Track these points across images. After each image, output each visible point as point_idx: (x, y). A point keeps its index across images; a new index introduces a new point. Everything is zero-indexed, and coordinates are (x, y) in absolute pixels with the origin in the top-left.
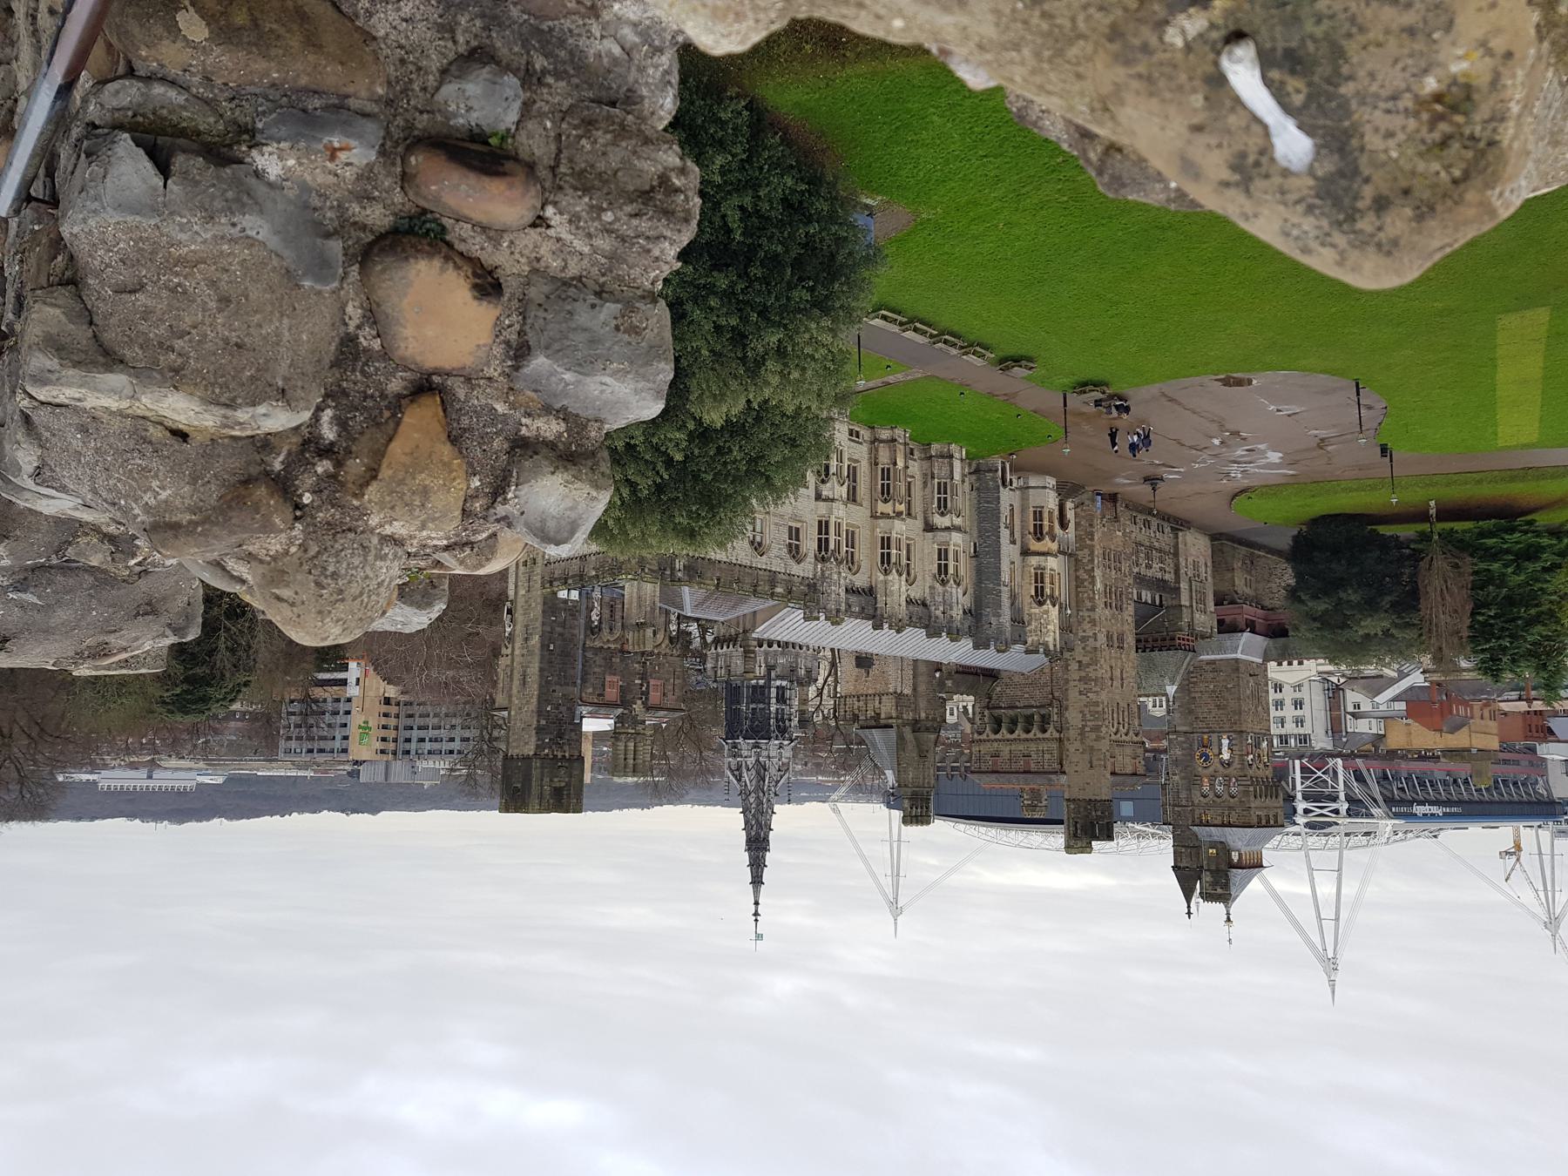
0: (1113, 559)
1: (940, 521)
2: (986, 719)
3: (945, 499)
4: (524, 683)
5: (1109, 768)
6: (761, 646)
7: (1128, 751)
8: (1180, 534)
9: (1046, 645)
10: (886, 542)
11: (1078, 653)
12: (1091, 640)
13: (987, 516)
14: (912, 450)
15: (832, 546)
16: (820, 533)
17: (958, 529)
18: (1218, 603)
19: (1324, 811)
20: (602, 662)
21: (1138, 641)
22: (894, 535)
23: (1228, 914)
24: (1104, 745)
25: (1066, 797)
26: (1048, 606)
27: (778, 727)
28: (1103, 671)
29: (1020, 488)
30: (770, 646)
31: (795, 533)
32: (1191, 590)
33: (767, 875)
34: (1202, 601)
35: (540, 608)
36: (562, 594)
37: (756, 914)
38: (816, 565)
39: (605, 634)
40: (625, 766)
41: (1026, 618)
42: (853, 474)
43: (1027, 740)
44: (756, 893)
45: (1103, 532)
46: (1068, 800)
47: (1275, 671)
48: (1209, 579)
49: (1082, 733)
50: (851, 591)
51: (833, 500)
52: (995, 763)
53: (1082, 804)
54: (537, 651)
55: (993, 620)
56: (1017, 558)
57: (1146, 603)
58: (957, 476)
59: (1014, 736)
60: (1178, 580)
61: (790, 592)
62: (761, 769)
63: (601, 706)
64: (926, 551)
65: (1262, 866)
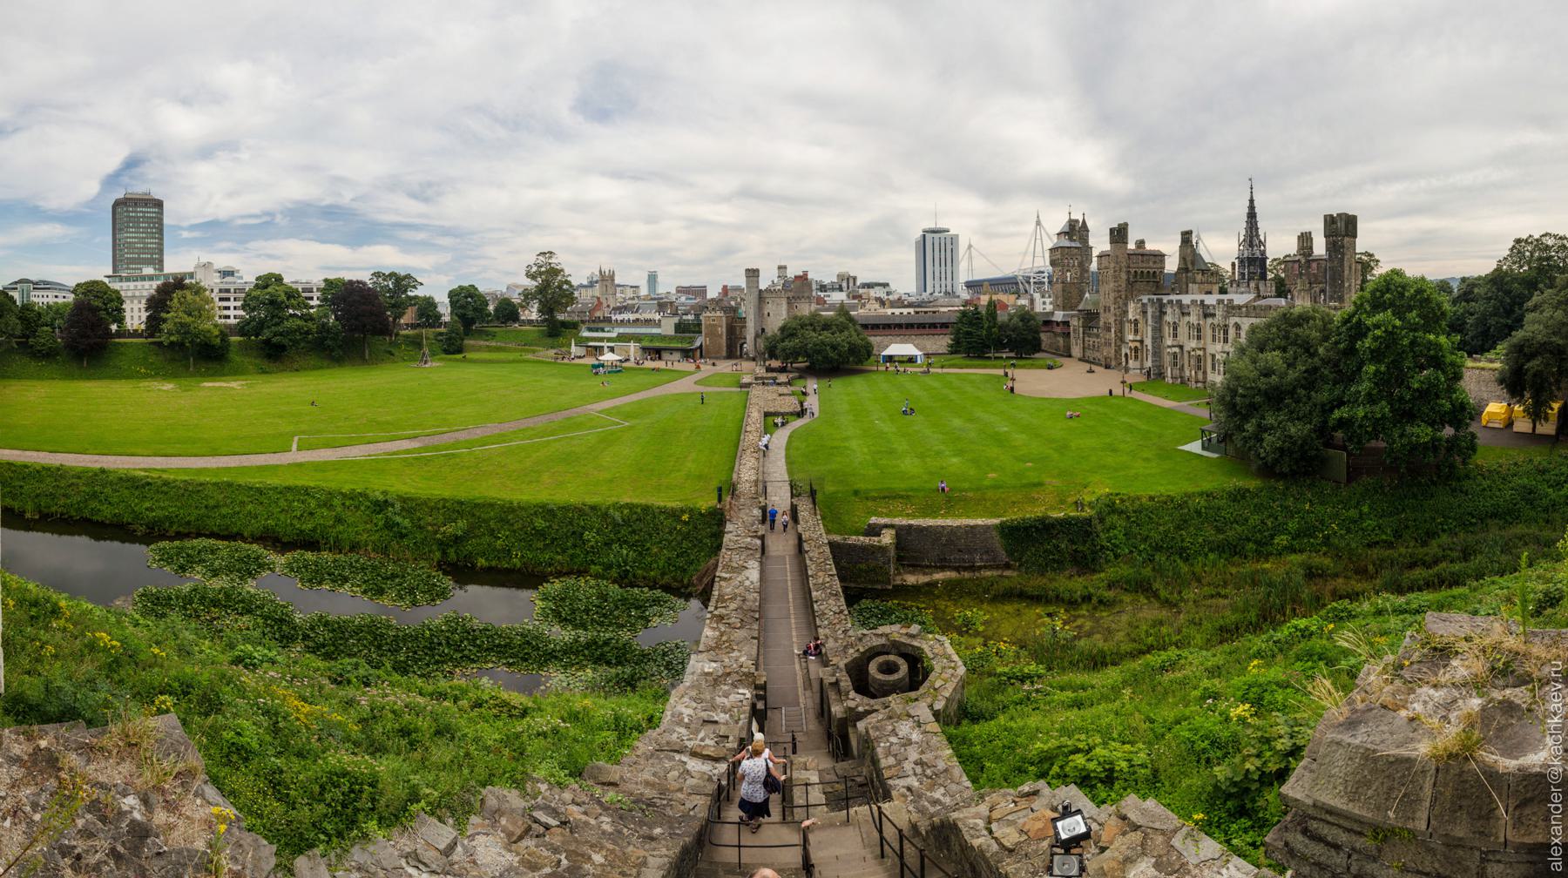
0: (1108, 344)
1: (1177, 350)
10: (1199, 338)
13: (1157, 353)
18: (1069, 333)
24: (1112, 265)
26: (1133, 319)
28: (1112, 295)
33: (1248, 204)
34: (1074, 330)
44: (1252, 197)
47: (1049, 308)
50: (1213, 315)
62: (1251, 245)
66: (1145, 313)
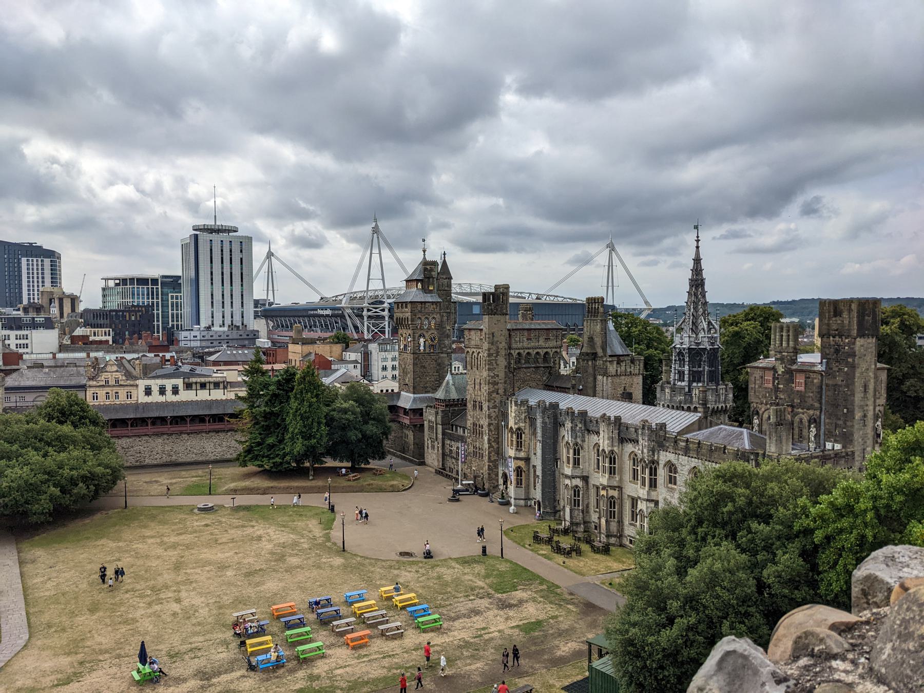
0: (477, 454)
1: (578, 482)
2: (552, 360)
3: (575, 496)
4: (865, 387)
5: (483, 333)
6: (696, 408)
7: (473, 343)
8: (441, 467)
9: (516, 405)
10: (612, 471)
11: (498, 399)
12: (491, 406)
14: (596, 528)
15: (647, 471)
16: (656, 479)
17: (567, 477)
18: (423, 425)
19: (374, 310)
20: (806, 399)
21: (465, 405)
22: (607, 475)
23: (424, 255)
25: (508, 317)
26: (515, 427)
27: (683, 356)
29: (530, 499)
30: (689, 408)
31: (672, 480)
32: (436, 434)
33: (691, 264)
34: (431, 428)
35: (856, 436)
36: (838, 447)
37: (698, 241)
38: (658, 457)
39: (805, 418)
40: (788, 331)
41: (528, 420)
42: (634, 516)
43: (529, 348)
45: (482, 469)
46: (507, 314)
47: (394, 386)
48: (426, 440)
49: (497, 353)
51: (647, 500)
52: (548, 335)
53: (498, 312)
54: (856, 409)
55: (547, 420)
56: (533, 457)
57: (460, 427)
58: (568, 510)
59: (536, 351)
60: (443, 439)
61: (676, 442)
62: (695, 329)
63: (807, 371)
64: (587, 464)
65: (407, 281)
66: (532, 422)
